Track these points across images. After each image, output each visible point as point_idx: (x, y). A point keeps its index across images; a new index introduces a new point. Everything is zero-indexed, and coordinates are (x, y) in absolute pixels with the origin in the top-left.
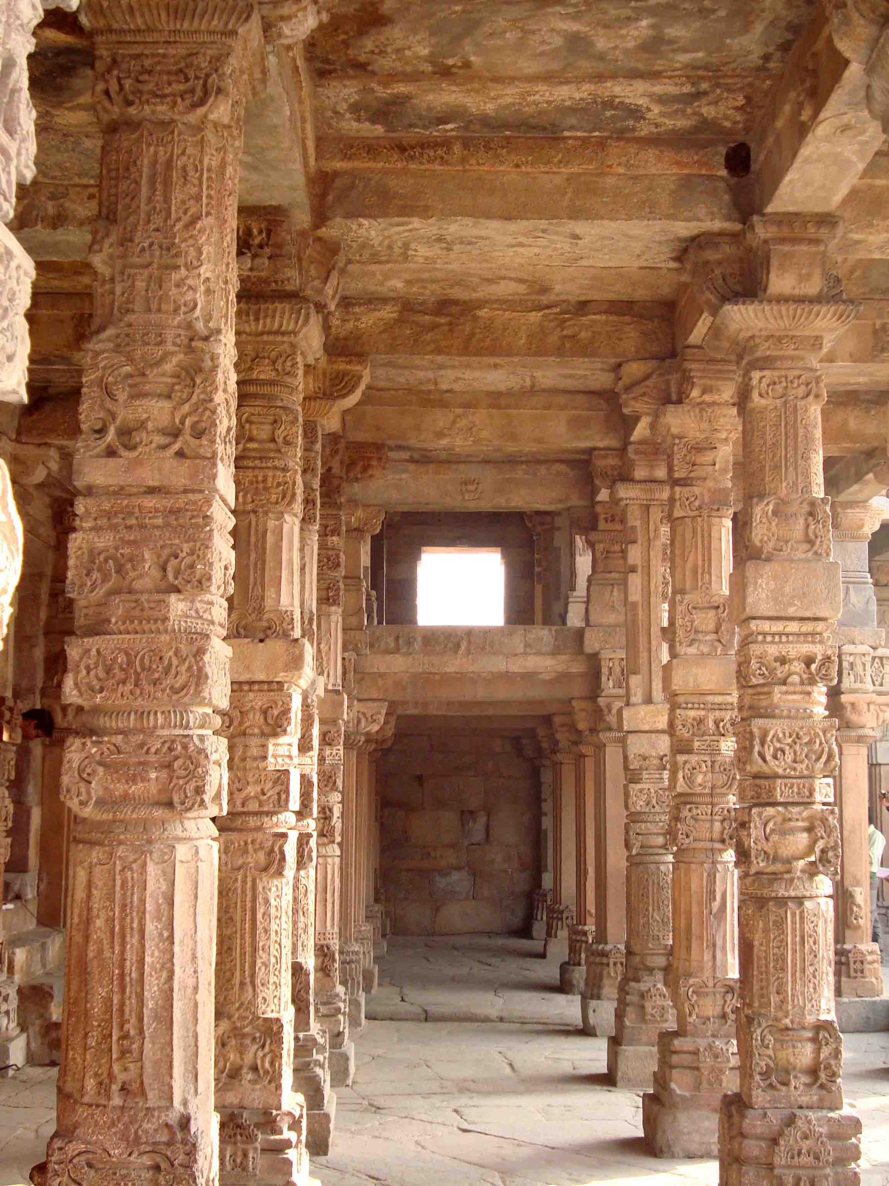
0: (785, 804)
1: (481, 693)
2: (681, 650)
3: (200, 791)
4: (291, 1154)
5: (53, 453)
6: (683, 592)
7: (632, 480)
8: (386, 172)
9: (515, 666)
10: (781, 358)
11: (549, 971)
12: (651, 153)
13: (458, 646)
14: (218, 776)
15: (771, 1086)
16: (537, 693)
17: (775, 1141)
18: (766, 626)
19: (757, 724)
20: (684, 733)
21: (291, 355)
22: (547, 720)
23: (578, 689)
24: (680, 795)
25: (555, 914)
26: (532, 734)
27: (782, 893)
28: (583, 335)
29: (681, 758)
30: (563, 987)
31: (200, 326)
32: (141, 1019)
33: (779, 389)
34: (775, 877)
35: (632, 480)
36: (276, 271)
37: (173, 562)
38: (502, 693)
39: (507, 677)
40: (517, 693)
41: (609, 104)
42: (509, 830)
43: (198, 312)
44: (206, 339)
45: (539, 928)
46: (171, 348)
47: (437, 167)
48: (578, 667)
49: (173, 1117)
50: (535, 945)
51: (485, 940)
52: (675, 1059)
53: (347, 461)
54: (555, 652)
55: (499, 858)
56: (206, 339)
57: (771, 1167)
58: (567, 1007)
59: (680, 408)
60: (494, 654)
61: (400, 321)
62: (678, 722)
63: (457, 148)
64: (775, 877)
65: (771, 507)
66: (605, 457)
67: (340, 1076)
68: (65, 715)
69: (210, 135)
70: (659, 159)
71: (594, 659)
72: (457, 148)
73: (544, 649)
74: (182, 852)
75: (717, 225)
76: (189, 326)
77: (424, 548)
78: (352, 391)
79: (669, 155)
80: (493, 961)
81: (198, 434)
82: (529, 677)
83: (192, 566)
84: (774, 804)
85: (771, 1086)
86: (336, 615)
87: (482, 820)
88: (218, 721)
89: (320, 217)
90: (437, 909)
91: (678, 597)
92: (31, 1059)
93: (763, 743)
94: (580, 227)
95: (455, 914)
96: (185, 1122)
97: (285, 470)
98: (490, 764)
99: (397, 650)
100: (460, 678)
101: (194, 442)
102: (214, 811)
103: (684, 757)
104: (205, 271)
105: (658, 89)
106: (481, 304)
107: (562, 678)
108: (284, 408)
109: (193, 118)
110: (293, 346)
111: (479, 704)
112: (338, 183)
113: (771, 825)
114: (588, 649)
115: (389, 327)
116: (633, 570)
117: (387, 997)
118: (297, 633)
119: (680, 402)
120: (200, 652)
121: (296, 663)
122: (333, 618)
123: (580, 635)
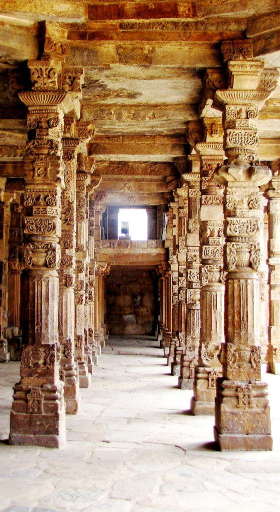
0: (195, 288)
1: (134, 260)
2: (180, 251)
3: (72, 283)
4: (84, 365)
5: (15, 194)
6: (181, 236)
7: (174, 201)
8: (104, 143)
9: (145, 252)
10: (196, 186)
11: (157, 343)
12: (166, 139)
13: (128, 246)
14: (74, 281)
15: (191, 351)
16: (152, 260)
17: (191, 362)
18: (191, 248)
19: (189, 270)
20: (181, 272)
21: (83, 186)
22: (157, 266)
23: (162, 258)
24: (180, 287)
25: (160, 327)
26: (154, 270)
27: (194, 308)
28: (156, 169)
29: (180, 278)
30: (161, 347)
31: (70, 201)
32: (62, 322)
33: (195, 193)
34: (193, 304)
35: (174, 201)
36: (80, 168)
37: (66, 243)
38: (140, 260)
39: (142, 255)
40: (145, 260)
41: (155, 130)
42: (148, 302)
43: (70, 198)
44: (72, 203)
45: (156, 332)
46: (65, 205)
47: (116, 142)
48: (162, 252)
49: (68, 339)
50: (156, 338)
51: (140, 336)
52: (177, 352)
53: (95, 196)
54: (156, 247)
55: (145, 310)
56: (72, 203)
57: (189, 367)
58: (160, 352)
59: (180, 189)
60: (138, 248)
61: (109, 166)
62: (180, 269)
63: (121, 138)
64: (193, 304)
65: (193, 221)
66: (167, 195)
67: (95, 362)
68: (15, 266)
69: (71, 165)
70: (168, 140)
71: (167, 250)
72: (121, 138)
73: (153, 247)
74: (69, 294)
75: (181, 155)
76: (69, 201)
77: (120, 209)
78: (97, 185)
79: (170, 139)
80: (141, 341)
81: (71, 221)
82: (148, 255)
83: (70, 244)
84: (192, 288)
85: (191, 351)
86: (93, 238)
87: (139, 298)
88: (74, 271)
89: (90, 153)
90: (124, 327)
91: (180, 237)
92: (11, 360)
93: (190, 274)
94: (150, 156)
95: (130, 329)
96: (70, 340)
97: (82, 212)
98: (142, 281)
99: (110, 247)
100: (129, 255)
101: (70, 222)
102: (73, 287)
103: (181, 278)
104: (71, 191)
105: (165, 129)
106: (130, 162)
107: (158, 255)
108: (82, 198)
109: (69, 162)
110: (84, 184)
111: (133, 263)
112: (94, 145)
113: (192, 293)
114: (166, 247)
115: (107, 168)
116: (174, 226)
117: (109, 348)
118: (85, 250)
119: (181, 187)
120: (71, 259)
121: (85, 257)
122: (92, 240)
123: (163, 242)
